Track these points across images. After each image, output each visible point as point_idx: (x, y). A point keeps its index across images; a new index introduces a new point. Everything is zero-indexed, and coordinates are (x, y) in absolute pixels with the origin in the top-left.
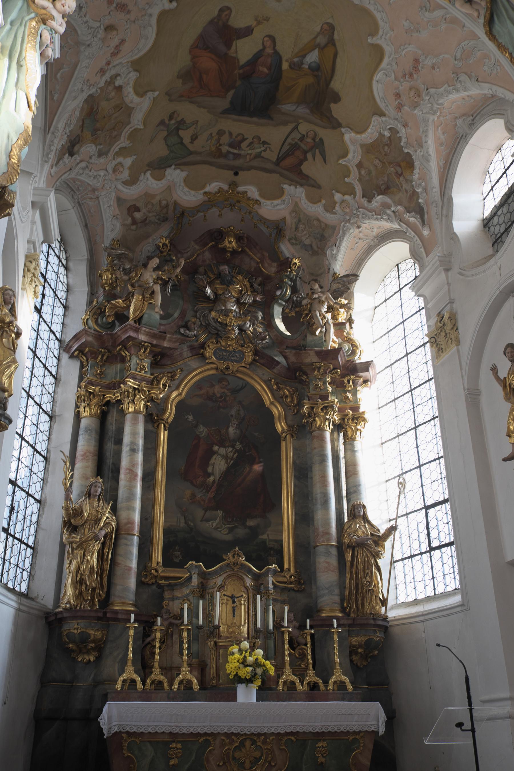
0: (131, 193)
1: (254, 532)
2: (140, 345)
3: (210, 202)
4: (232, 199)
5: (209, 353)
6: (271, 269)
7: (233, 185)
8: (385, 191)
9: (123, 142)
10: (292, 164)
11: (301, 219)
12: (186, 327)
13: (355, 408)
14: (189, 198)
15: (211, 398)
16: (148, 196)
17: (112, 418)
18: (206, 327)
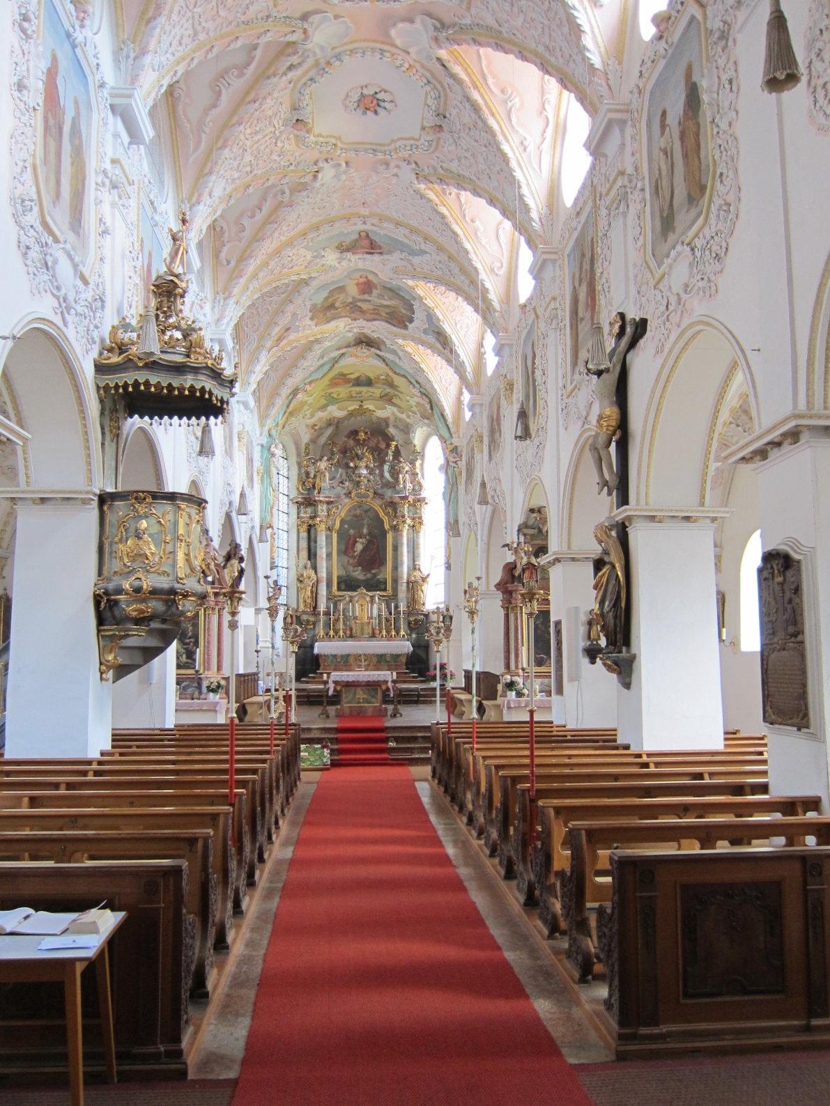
0: (311, 422)
1: (375, 575)
2: (321, 501)
3: (351, 414)
4: (361, 411)
5: (353, 495)
6: (383, 446)
7: (361, 406)
8: (428, 419)
9: (306, 407)
10: (388, 399)
11: (396, 419)
12: (342, 482)
13: (420, 518)
14: (339, 414)
15: (355, 516)
16: (320, 419)
17: (313, 531)
18: (351, 481)
